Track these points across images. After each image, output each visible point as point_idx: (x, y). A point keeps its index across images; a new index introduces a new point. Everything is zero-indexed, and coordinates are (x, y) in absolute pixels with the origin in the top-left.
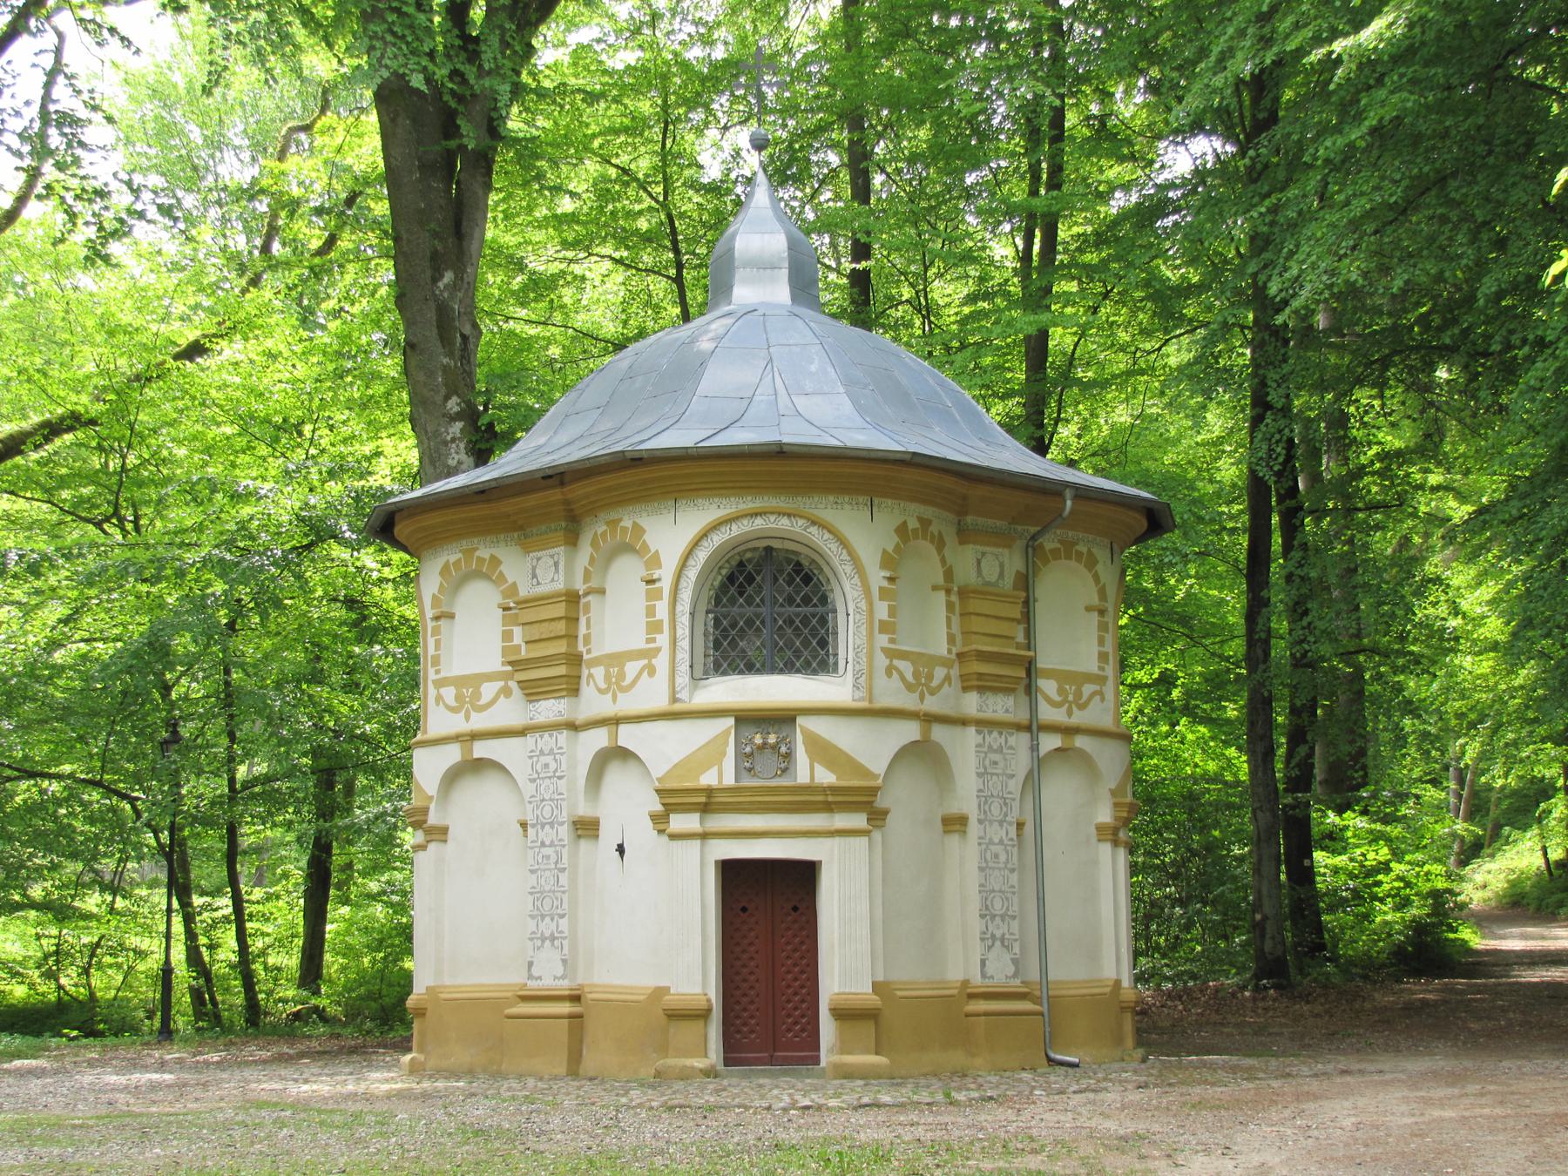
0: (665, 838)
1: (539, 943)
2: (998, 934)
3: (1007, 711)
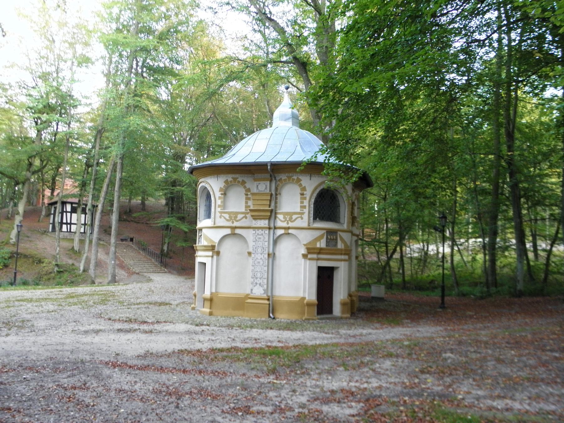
2: (258, 282)
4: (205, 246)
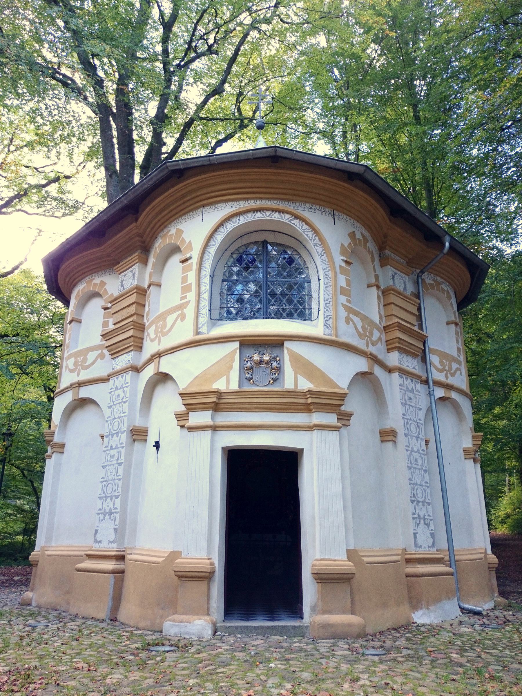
0: (186, 431)
1: (102, 516)
3: (414, 368)
4: (304, 394)
